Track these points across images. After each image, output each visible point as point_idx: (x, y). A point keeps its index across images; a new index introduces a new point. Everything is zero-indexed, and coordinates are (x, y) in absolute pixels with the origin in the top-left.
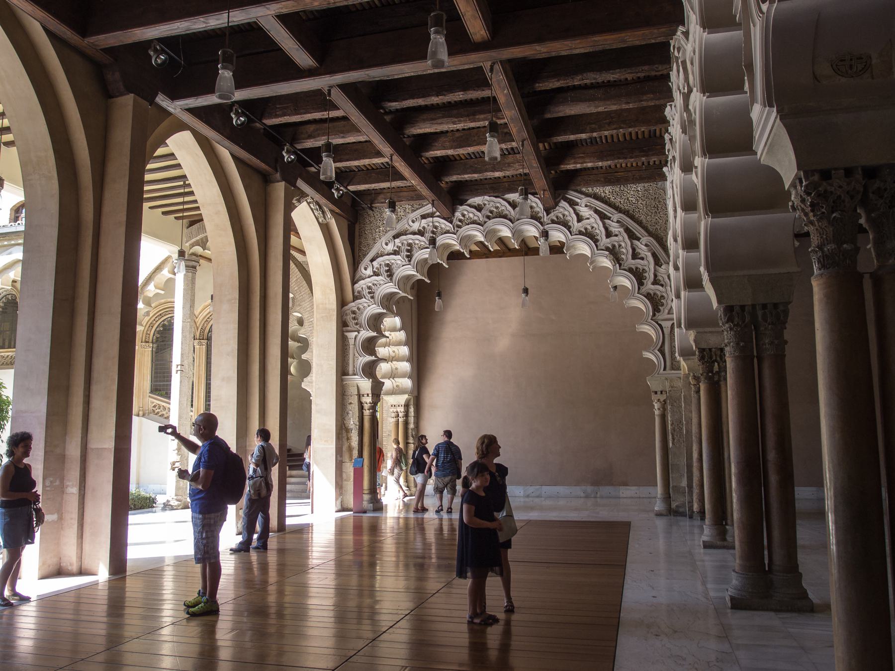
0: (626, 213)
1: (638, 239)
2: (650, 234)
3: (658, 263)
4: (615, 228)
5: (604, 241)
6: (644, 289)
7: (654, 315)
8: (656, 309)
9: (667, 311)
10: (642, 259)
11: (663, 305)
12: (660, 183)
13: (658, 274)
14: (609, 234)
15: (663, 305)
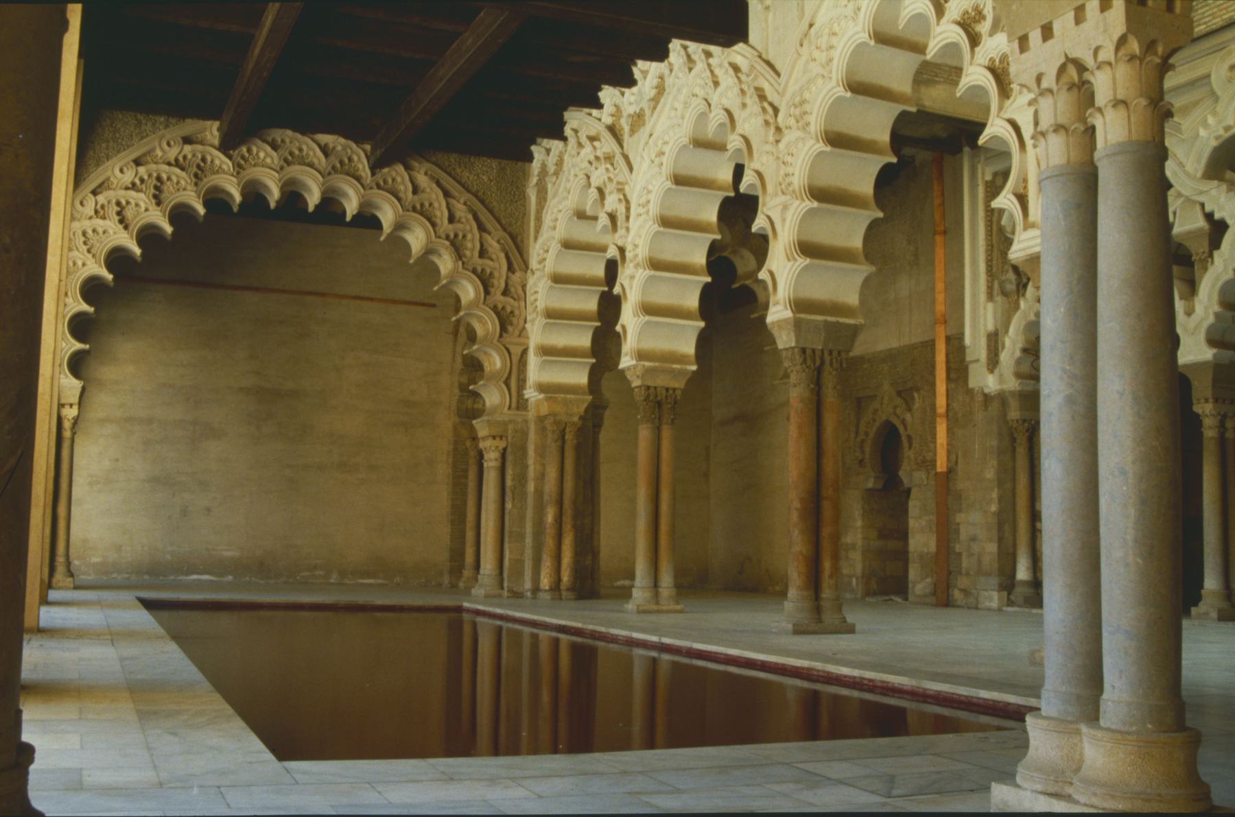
0: (475, 195)
1: (489, 234)
2: (505, 230)
3: (511, 268)
4: (461, 210)
5: (444, 226)
6: (490, 300)
7: (501, 336)
8: (503, 329)
9: (517, 332)
10: (492, 260)
11: (511, 324)
12: (520, 164)
13: (510, 283)
14: (451, 219)
15: (511, 324)
